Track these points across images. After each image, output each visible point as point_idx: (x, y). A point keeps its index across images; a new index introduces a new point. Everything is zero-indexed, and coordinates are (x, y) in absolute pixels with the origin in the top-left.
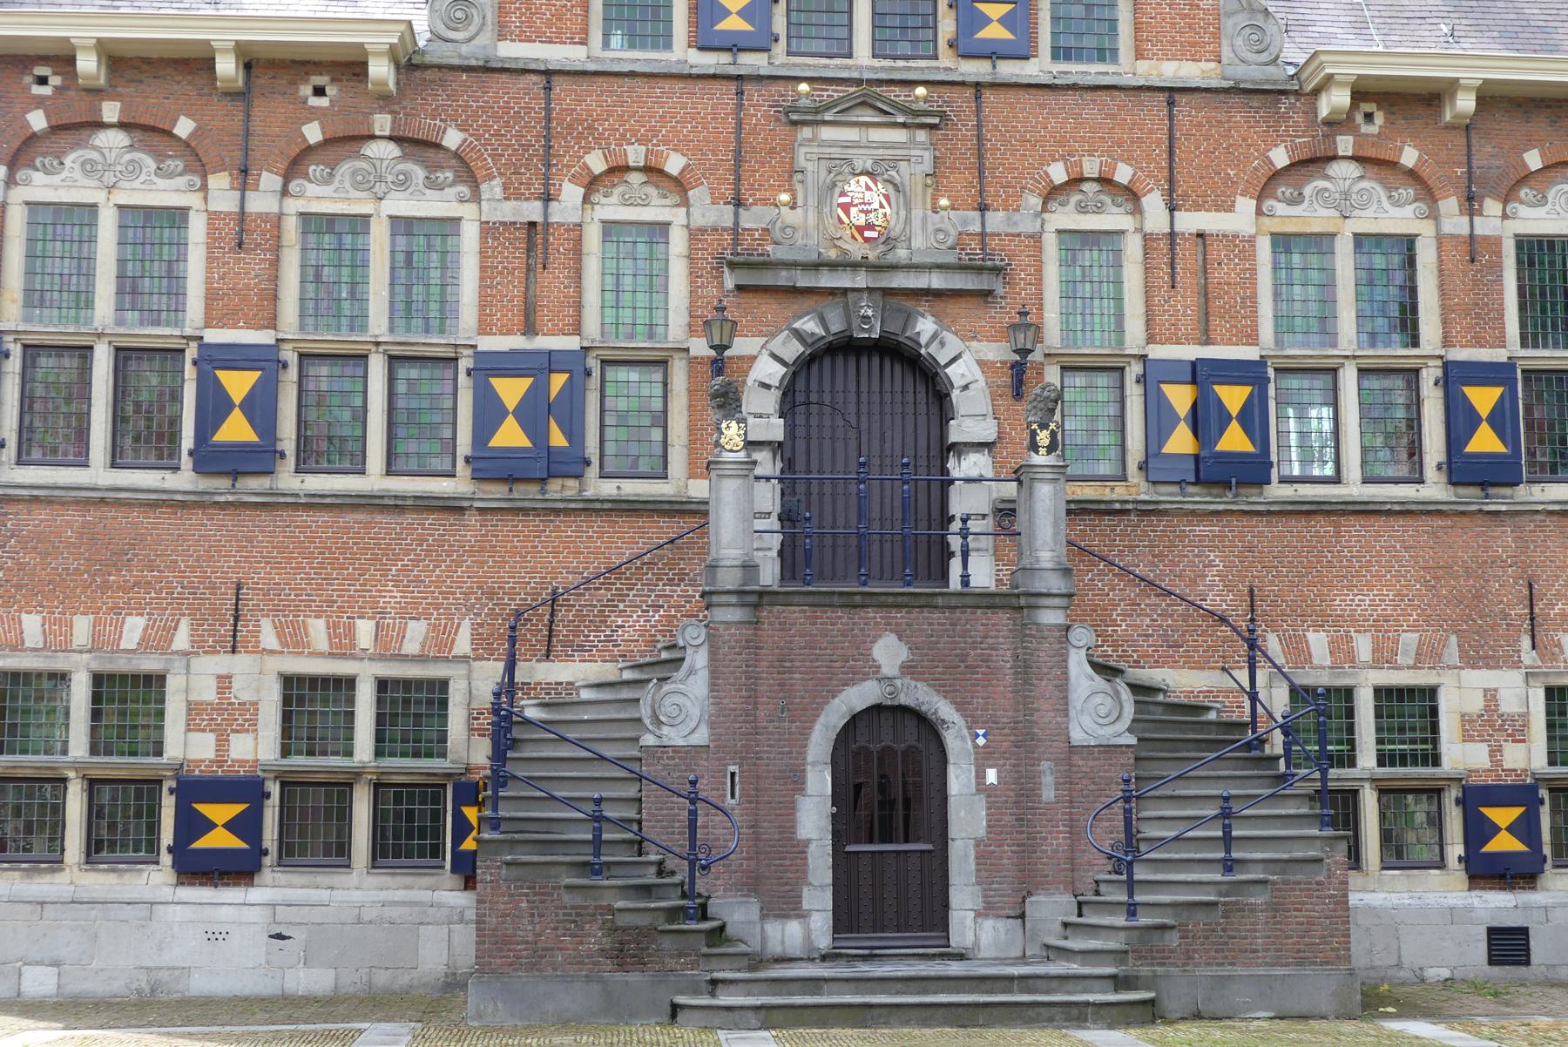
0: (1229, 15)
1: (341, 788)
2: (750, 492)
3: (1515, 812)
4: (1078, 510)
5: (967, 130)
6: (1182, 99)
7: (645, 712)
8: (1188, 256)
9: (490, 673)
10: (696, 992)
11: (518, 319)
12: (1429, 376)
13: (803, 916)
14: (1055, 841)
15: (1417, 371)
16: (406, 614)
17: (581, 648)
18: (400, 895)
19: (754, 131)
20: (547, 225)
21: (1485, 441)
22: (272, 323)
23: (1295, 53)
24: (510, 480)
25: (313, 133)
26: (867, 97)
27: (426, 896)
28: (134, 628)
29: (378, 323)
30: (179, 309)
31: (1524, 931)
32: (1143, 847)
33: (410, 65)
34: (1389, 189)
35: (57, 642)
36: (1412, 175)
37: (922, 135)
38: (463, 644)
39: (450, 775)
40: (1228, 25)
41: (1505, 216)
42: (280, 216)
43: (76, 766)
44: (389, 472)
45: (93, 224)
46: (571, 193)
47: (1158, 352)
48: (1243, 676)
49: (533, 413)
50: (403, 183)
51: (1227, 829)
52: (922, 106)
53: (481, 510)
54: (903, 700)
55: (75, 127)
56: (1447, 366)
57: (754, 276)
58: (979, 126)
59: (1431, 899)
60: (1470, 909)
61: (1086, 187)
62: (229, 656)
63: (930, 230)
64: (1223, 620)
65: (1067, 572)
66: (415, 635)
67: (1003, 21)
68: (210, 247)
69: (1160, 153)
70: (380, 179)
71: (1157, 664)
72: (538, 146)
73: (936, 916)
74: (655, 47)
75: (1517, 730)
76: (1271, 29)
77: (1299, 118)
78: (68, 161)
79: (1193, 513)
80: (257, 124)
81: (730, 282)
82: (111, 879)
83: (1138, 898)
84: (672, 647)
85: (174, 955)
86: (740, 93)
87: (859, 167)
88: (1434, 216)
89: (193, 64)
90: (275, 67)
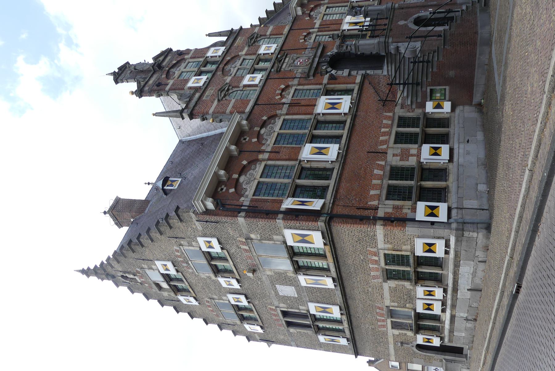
27: (456, 118)
38: (391, 114)
46: (284, 100)
53: (357, 111)
62: (388, 155)
72: (272, 103)
78: (244, 187)
81: (312, 78)
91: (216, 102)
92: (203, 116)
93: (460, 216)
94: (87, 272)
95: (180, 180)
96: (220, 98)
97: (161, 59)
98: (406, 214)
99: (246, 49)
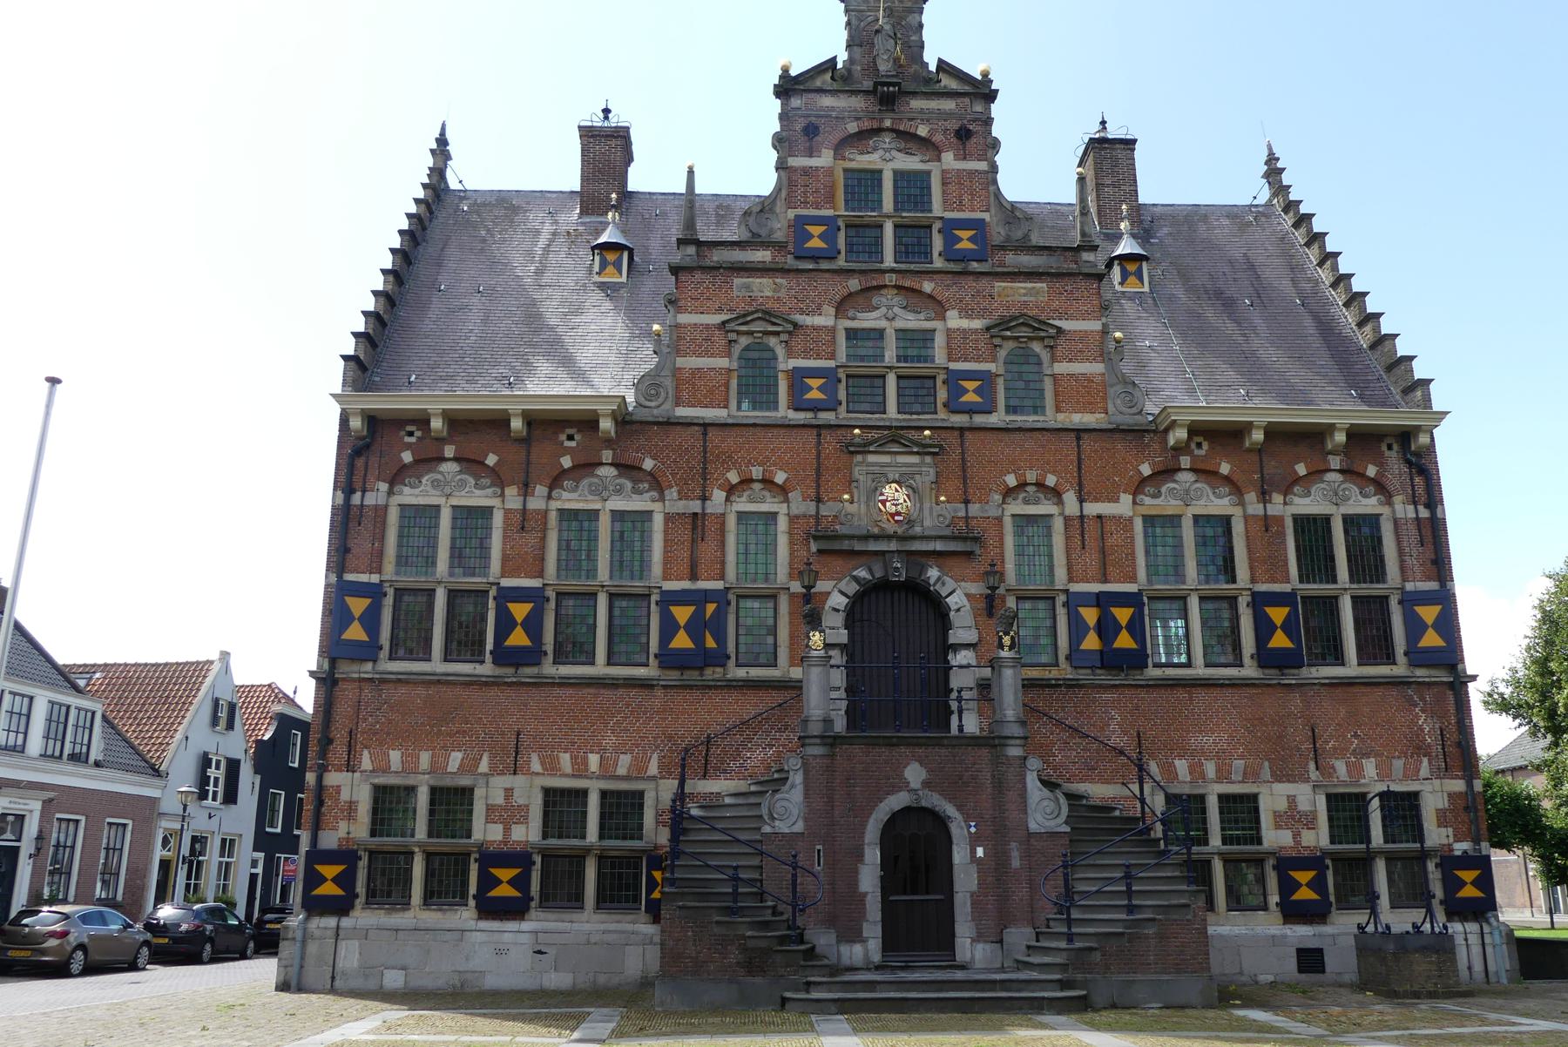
0: (1112, 386)
1: (578, 858)
2: (828, 674)
3: (1311, 874)
4: (1029, 685)
5: (955, 455)
6: (1086, 436)
7: (764, 811)
8: (1092, 530)
9: (669, 787)
10: (797, 990)
11: (687, 571)
12: (1243, 601)
13: (863, 941)
14: (1021, 893)
15: (1236, 598)
16: (619, 750)
17: (725, 771)
18: (613, 927)
19: (828, 457)
20: (704, 514)
21: (1280, 641)
22: (541, 574)
23: (1152, 408)
24: (682, 668)
25: (566, 462)
26: (895, 437)
27: (629, 927)
28: (456, 758)
29: (603, 574)
30: (487, 566)
31: (1320, 951)
32: (1076, 897)
33: (624, 420)
34: (1213, 488)
35: (410, 767)
36: (1227, 480)
37: (928, 459)
38: (653, 769)
39: (644, 851)
40: (1111, 391)
41: (1285, 503)
42: (546, 511)
43: (420, 844)
44: (609, 663)
45: (437, 517)
46: (718, 496)
47: (1076, 588)
48: (1135, 788)
49: (696, 628)
50: (619, 491)
51: (1129, 886)
52: (928, 441)
54: (924, 804)
55: (428, 460)
56: (1254, 595)
57: (828, 544)
58: (963, 453)
59: (1259, 930)
60: (1285, 936)
61: (1029, 488)
63: (938, 513)
64: (1122, 753)
65: (1023, 723)
66: (624, 763)
67: (975, 391)
68: (505, 530)
69: (1073, 468)
70: (606, 488)
71: (1082, 781)
73: (944, 941)
74: (768, 409)
75: (1310, 821)
76: (1137, 393)
77: (1156, 446)
78: (424, 480)
79: (1100, 686)
80: (533, 457)
81: (814, 548)
82: (439, 915)
83: (1074, 930)
84: (781, 771)
85: (476, 964)
86: (819, 435)
87: (891, 476)
88: (1242, 504)
89: (496, 423)
90: (547, 424)
91: (717, 319)
92: (670, 302)
93: (317, 933)
94: (442, 149)
95: (624, 279)
96: (732, 326)
97: (948, 82)
98: (335, 829)
99: (977, 324)
